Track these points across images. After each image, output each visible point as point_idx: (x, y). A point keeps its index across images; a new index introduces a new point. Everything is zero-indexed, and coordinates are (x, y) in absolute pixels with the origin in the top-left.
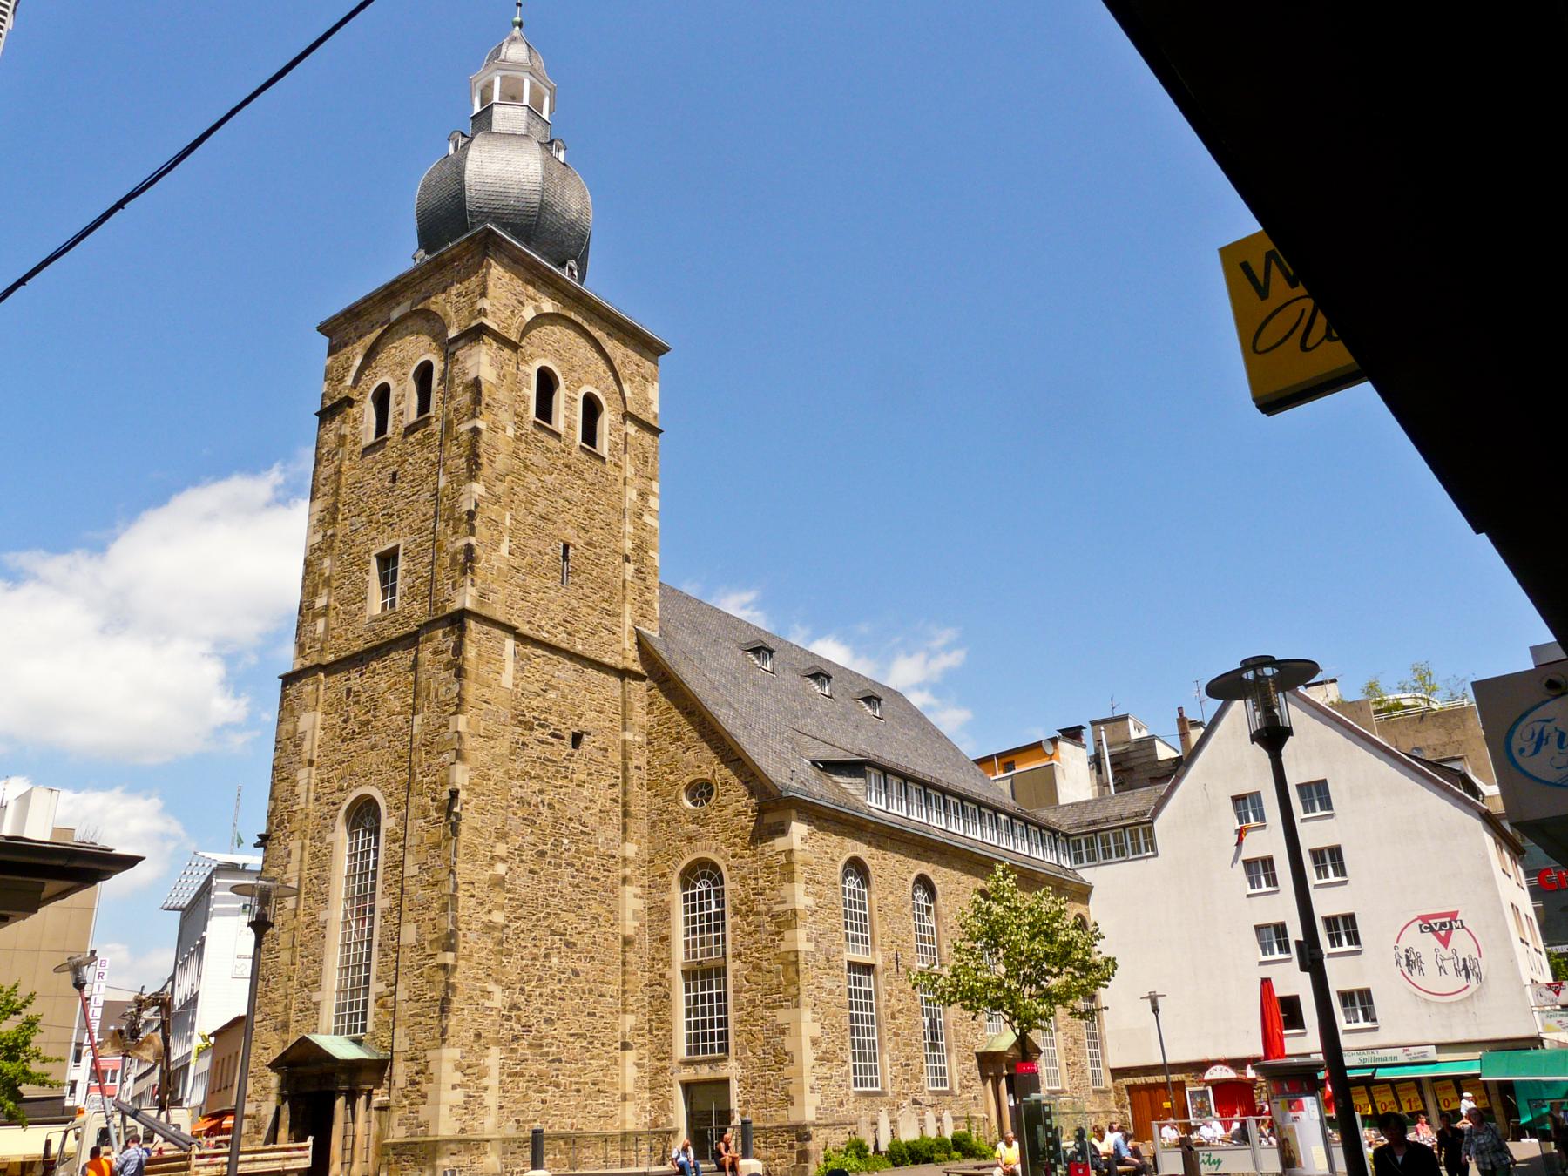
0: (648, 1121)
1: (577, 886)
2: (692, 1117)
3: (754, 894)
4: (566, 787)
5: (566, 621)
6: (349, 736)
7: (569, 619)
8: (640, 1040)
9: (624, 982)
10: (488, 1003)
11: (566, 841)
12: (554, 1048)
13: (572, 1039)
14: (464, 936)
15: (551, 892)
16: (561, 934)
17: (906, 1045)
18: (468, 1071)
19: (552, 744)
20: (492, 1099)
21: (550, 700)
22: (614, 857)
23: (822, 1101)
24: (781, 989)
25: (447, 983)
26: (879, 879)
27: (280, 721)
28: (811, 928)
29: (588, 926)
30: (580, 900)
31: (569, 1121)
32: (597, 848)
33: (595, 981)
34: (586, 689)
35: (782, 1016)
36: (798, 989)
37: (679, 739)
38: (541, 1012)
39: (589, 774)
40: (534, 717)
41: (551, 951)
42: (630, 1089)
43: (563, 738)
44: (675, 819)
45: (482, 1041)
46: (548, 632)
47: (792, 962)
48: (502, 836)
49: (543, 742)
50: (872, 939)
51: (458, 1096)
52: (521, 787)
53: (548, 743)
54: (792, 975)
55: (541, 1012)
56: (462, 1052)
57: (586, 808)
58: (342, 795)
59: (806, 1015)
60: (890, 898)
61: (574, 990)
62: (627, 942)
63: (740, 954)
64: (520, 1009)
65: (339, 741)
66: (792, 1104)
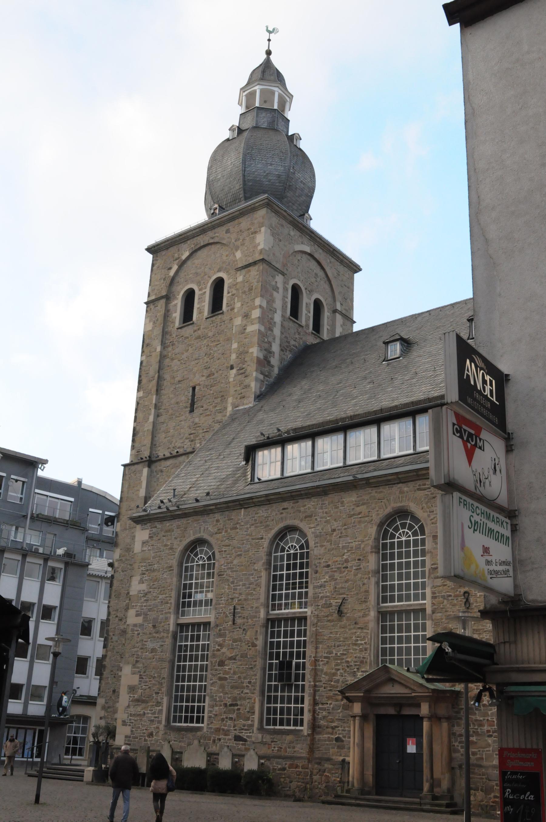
14: (112, 638)
23: (132, 731)
56: (106, 700)
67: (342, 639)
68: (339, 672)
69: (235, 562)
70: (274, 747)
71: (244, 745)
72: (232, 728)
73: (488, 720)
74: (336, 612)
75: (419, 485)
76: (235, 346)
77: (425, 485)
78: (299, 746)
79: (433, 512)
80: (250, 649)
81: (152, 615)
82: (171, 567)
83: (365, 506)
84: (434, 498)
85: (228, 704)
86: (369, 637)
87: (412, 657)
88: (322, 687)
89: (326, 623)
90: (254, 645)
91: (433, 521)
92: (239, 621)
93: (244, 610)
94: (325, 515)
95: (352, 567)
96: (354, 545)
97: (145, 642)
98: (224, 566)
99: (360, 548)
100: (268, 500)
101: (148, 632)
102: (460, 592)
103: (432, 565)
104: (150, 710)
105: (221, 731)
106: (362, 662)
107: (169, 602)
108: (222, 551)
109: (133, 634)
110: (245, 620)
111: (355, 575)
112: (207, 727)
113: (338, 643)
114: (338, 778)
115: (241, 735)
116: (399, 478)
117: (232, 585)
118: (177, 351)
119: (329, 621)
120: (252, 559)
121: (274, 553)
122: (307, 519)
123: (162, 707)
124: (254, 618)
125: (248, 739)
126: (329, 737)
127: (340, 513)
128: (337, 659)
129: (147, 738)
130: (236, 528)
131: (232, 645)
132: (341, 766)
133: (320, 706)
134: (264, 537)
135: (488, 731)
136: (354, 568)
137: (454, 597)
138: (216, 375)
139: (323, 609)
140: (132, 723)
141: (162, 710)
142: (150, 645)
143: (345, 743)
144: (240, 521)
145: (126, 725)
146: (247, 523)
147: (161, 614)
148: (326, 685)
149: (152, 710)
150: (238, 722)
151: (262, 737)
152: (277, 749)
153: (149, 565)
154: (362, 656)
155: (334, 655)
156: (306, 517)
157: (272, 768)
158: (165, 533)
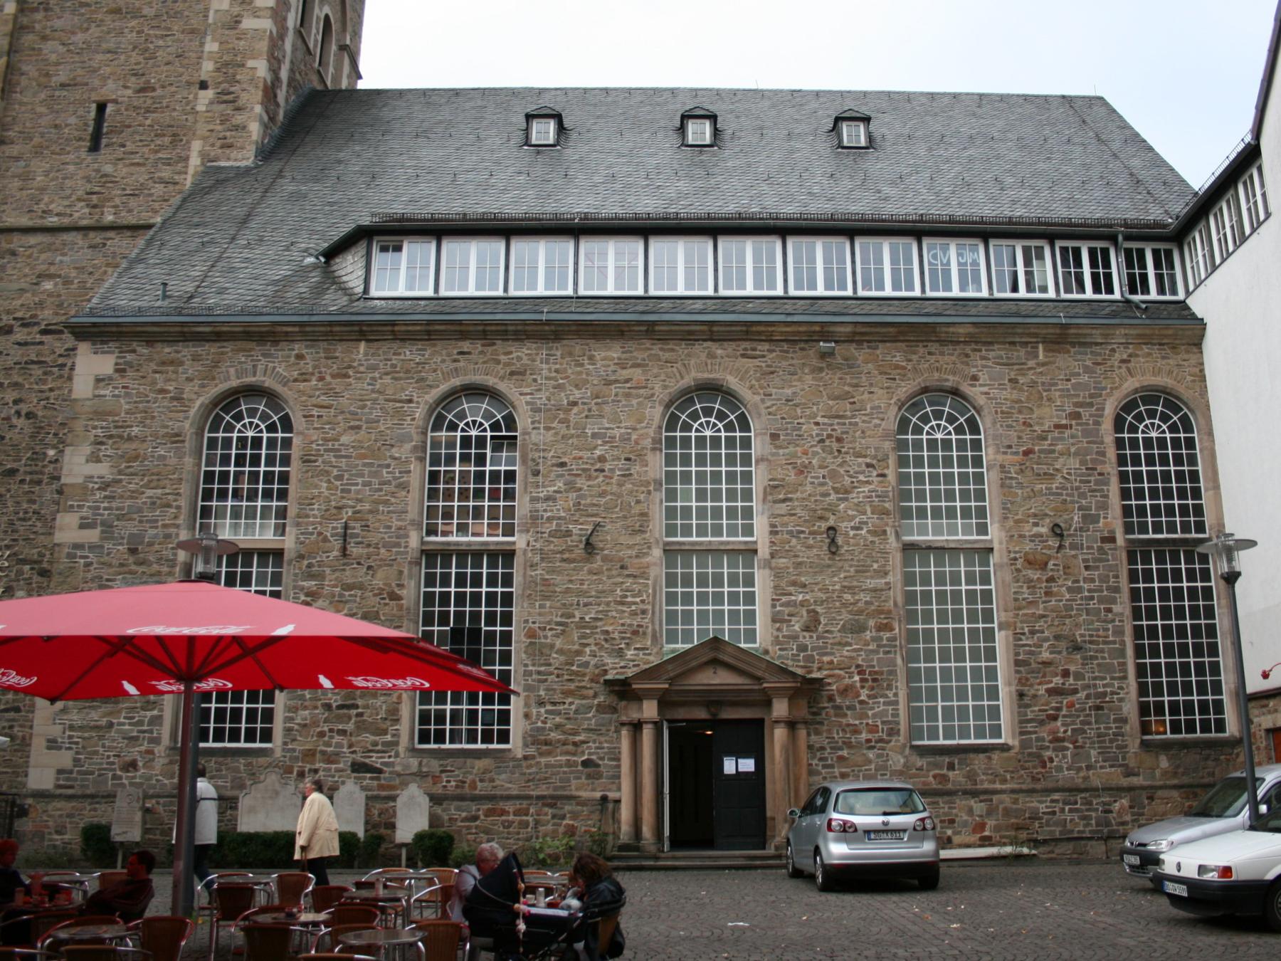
4: (59, 388)
11: (51, 453)
15: (21, 515)
19: (41, 343)
41: (14, 584)
49: (26, 344)
67: (594, 593)
68: (587, 650)
69: (345, 439)
70: (448, 781)
71: (378, 779)
72: (345, 750)
73: (867, 724)
74: (582, 546)
75: (745, 349)
76: (211, 46)
77: (754, 349)
78: (503, 776)
79: (771, 395)
80: (386, 604)
81: (127, 529)
82: (177, 435)
83: (639, 371)
84: (772, 373)
85: (334, 705)
86: (650, 591)
87: (695, 627)
88: (551, 674)
89: (558, 564)
90: (394, 597)
91: (770, 410)
92: (354, 550)
93: (369, 531)
94: (554, 374)
95: (612, 470)
96: (617, 432)
97: (108, 580)
98: (318, 445)
99: (629, 439)
100: (429, 333)
101: (115, 562)
102: (820, 527)
103: (770, 480)
104: (125, 718)
105: (318, 755)
106: (635, 633)
107: (175, 504)
108: (312, 416)
109: (72, 565)
110: (371, 549)
111: (620, 485)
112: (283, 750)
113: (586, 600)
114: (594, 826)
115: (367, 761)
116: (711, 332)
117: (338, 483)
118: (58, 23)
119: (564, 560)
120: (388, 438)
121: (433, 431)
122: (515, 377)
123: (162, 710)
124: (394, 547)
125: (385, 769)
126: (569, 760)
127: (587, 374)
128: (584, 627)
129: (119, 773)
130: (346, 376)
131: (341, 595)
132: (600, 807)
133: (549, 707)
134: (415, 399)
135: (868, 741)
136: (618, 473)
137: (810, 533)
138: (159, 92)
139: (552, 539)
140: (77, 743)
141: (161, 717)
143: (602, 769)
144: (355, 364)
145: (60, 748)
146: (373, 368)
147: (151, 527)
148: (560, 672)
149: (134, 718)
150: (360, 738)
151: (420, 764)
152: (453, 783)
153: (116, 427)
154: (636, 623)
155: (577, 619)
156: (512, 373)
157: (446, 818)
158: (157, 365)
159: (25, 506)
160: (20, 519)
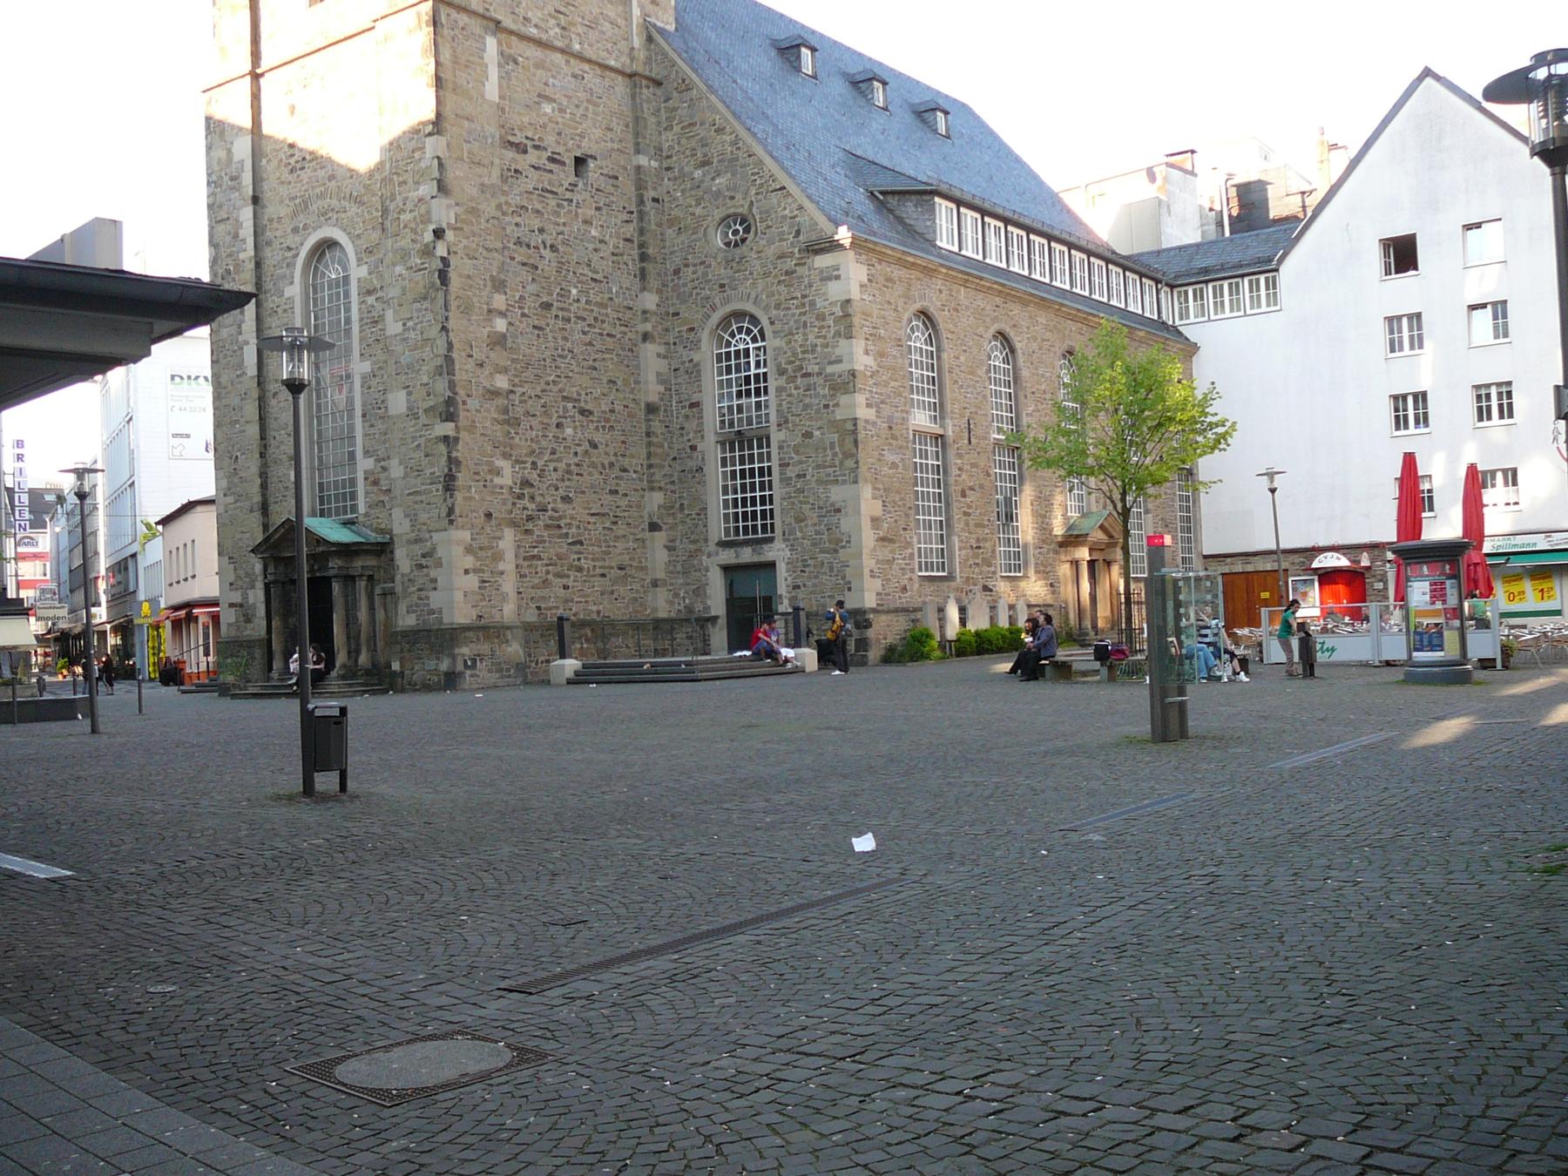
0: (681, 608)
1: (590, 344)
2: (731, 602)
3: (803, 352)
5: (559, 12)
6: (298, 166)
7: (562, 9)
8: (670, 520)
9: (649, 455)
10: (497, 480)
12: (574, 530)
13: (592, 520)
14: (464, 403)
16: (576, 400)
17: (977, 525)
18: (481, 554)
19: (551, 171)
20: (509, 585)
21: (545, 114)
22: (631, 309)
24: (837, 463)
25: (449, 458)
26: (950, 336)
27: (209, 148)
28: (871, 392)
29: (605, 391)
30: (595, 360)
31: (594, 608)
32: (611, 299)
33: (615, 454)
34: (588, 101)
35: (837, 494)
36: (857, 462)
37: (706, 163)
38: (557, 489)
39: (598, 209)
40: (527, 138)
42: (661, 575)
43: (563, 164)
44: (702, 263)
45: (493, 522)
46: (536, 26)
47: (850, 431)
48: (499, 285)
50: (942, 405)
51: (472, 582)
52: (517, 224)
53: (545, 170)
54: (849, 445)
55: (557, 489)
57: (596, 250)
58: (297, 239)
59: (866, 492)
60: (962, 359)
61: (593, 465)
62: (651, 409)
63: (786, 422)
64: (532, 486)
65: (286, 171)
66: (849, 589)
81: (887, 410)
142: (891, 457)
159: (561, 342)
160: (559, 356)
